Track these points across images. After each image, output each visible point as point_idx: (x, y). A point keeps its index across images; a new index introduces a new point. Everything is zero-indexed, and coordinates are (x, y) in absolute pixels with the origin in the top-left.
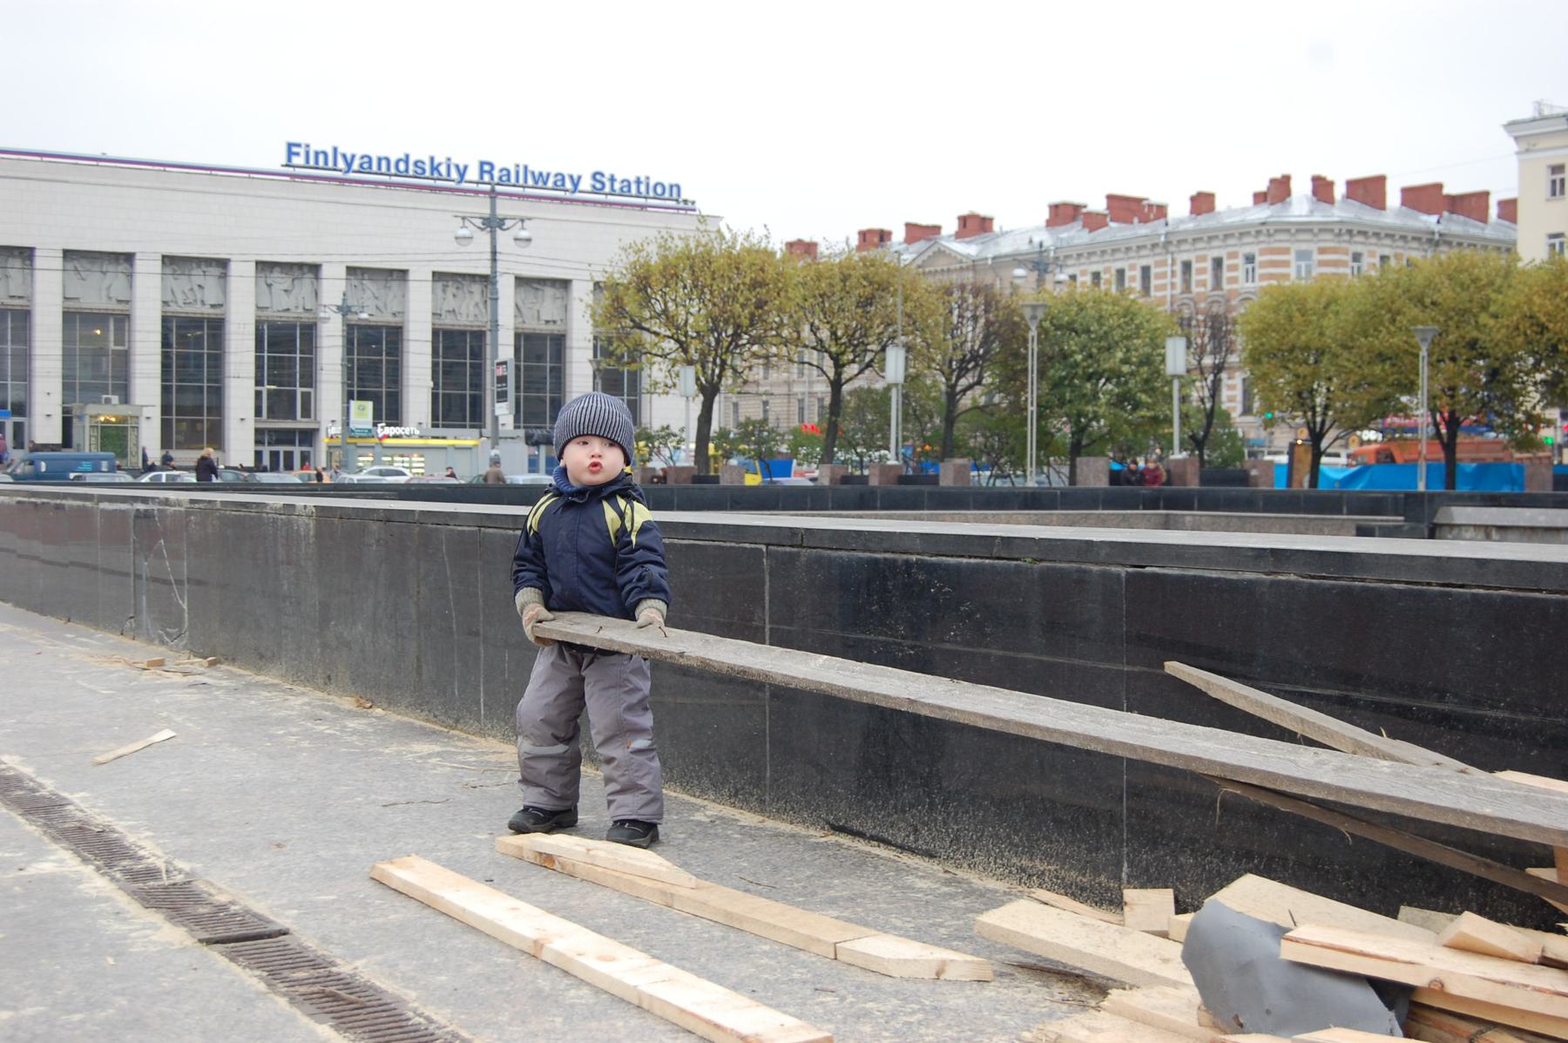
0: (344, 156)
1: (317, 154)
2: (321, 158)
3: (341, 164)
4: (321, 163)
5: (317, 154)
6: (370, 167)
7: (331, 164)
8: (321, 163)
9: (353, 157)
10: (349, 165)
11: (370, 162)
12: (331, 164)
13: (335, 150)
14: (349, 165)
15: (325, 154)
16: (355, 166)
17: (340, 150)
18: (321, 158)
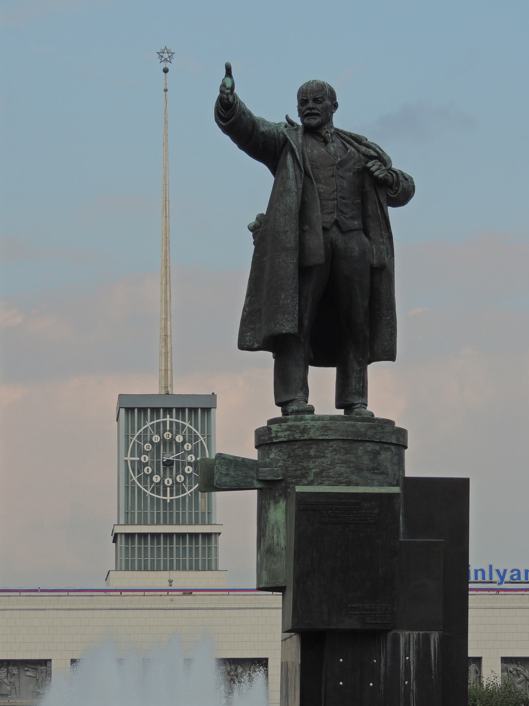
0: (498, 571)
1: (476, 571)
2: (480, 574)
3: (496, 578)
4: (480, 579)
5: (476, 571)
6: (519, 578)
7: (487, 579)
8: (480, 579)
9: (505, 571)
10: (502, 578)
11: (519, 574)
12: (487, 579)
13: (491, 567)
14: (502, 578)
15: (483, 571)
16: (507, 578)
17: (494, 568)
18: (480, 574)
